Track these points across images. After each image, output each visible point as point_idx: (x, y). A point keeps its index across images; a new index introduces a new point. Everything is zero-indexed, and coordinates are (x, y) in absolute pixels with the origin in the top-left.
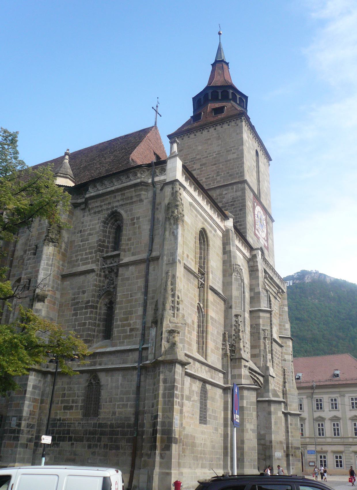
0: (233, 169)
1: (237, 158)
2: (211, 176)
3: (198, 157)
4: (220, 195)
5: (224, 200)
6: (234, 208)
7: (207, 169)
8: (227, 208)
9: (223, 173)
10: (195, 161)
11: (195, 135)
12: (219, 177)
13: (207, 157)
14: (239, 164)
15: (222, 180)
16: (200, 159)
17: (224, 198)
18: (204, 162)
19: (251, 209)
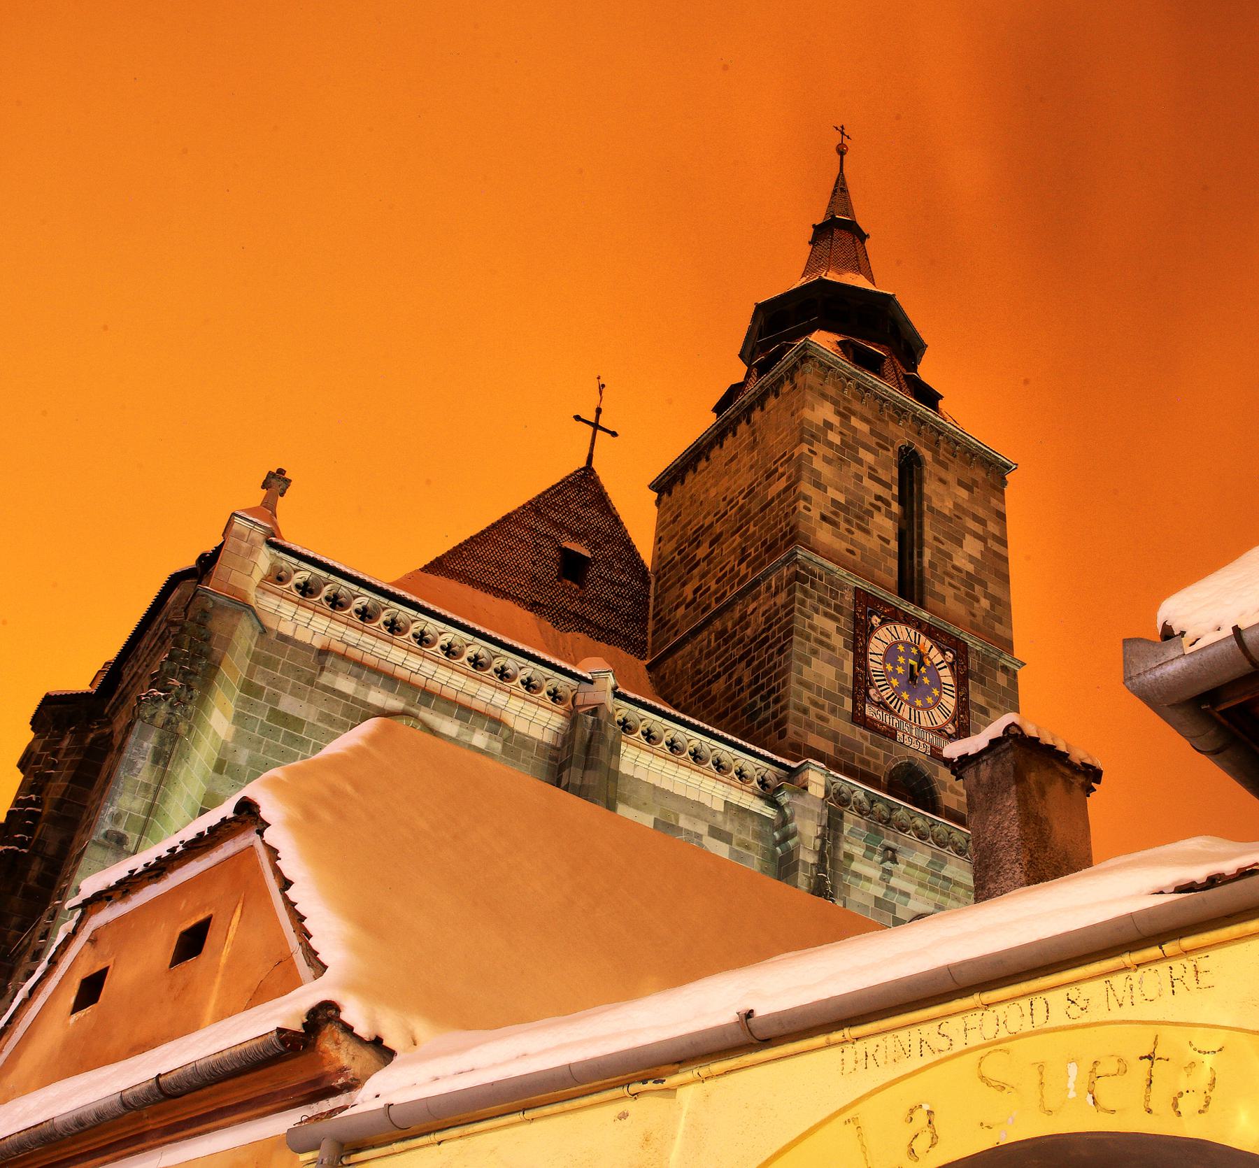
0: (776, 524)
1: (787, 489)
2: (727, 568)
3: (707, 522)
4: (743, 617)
5: (749, 632)
6: (770, 647)
7: (722, 550)
8: (752, 654)
9: (753, 549)
10: (700, 538)
11: (708, 459)
12: (744, 564)
13: (726, 513)
14: (789, 506)
15: (750, 569)
16: (711, 525)
17: (747, 626)
18: (718, 531)
19: (838, 641)
